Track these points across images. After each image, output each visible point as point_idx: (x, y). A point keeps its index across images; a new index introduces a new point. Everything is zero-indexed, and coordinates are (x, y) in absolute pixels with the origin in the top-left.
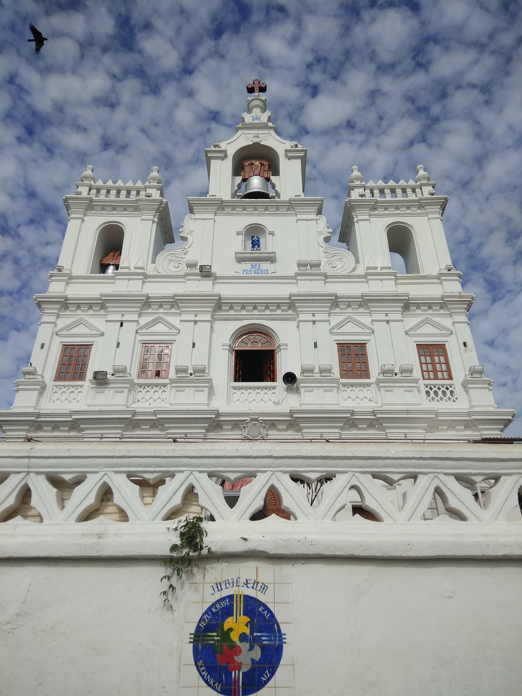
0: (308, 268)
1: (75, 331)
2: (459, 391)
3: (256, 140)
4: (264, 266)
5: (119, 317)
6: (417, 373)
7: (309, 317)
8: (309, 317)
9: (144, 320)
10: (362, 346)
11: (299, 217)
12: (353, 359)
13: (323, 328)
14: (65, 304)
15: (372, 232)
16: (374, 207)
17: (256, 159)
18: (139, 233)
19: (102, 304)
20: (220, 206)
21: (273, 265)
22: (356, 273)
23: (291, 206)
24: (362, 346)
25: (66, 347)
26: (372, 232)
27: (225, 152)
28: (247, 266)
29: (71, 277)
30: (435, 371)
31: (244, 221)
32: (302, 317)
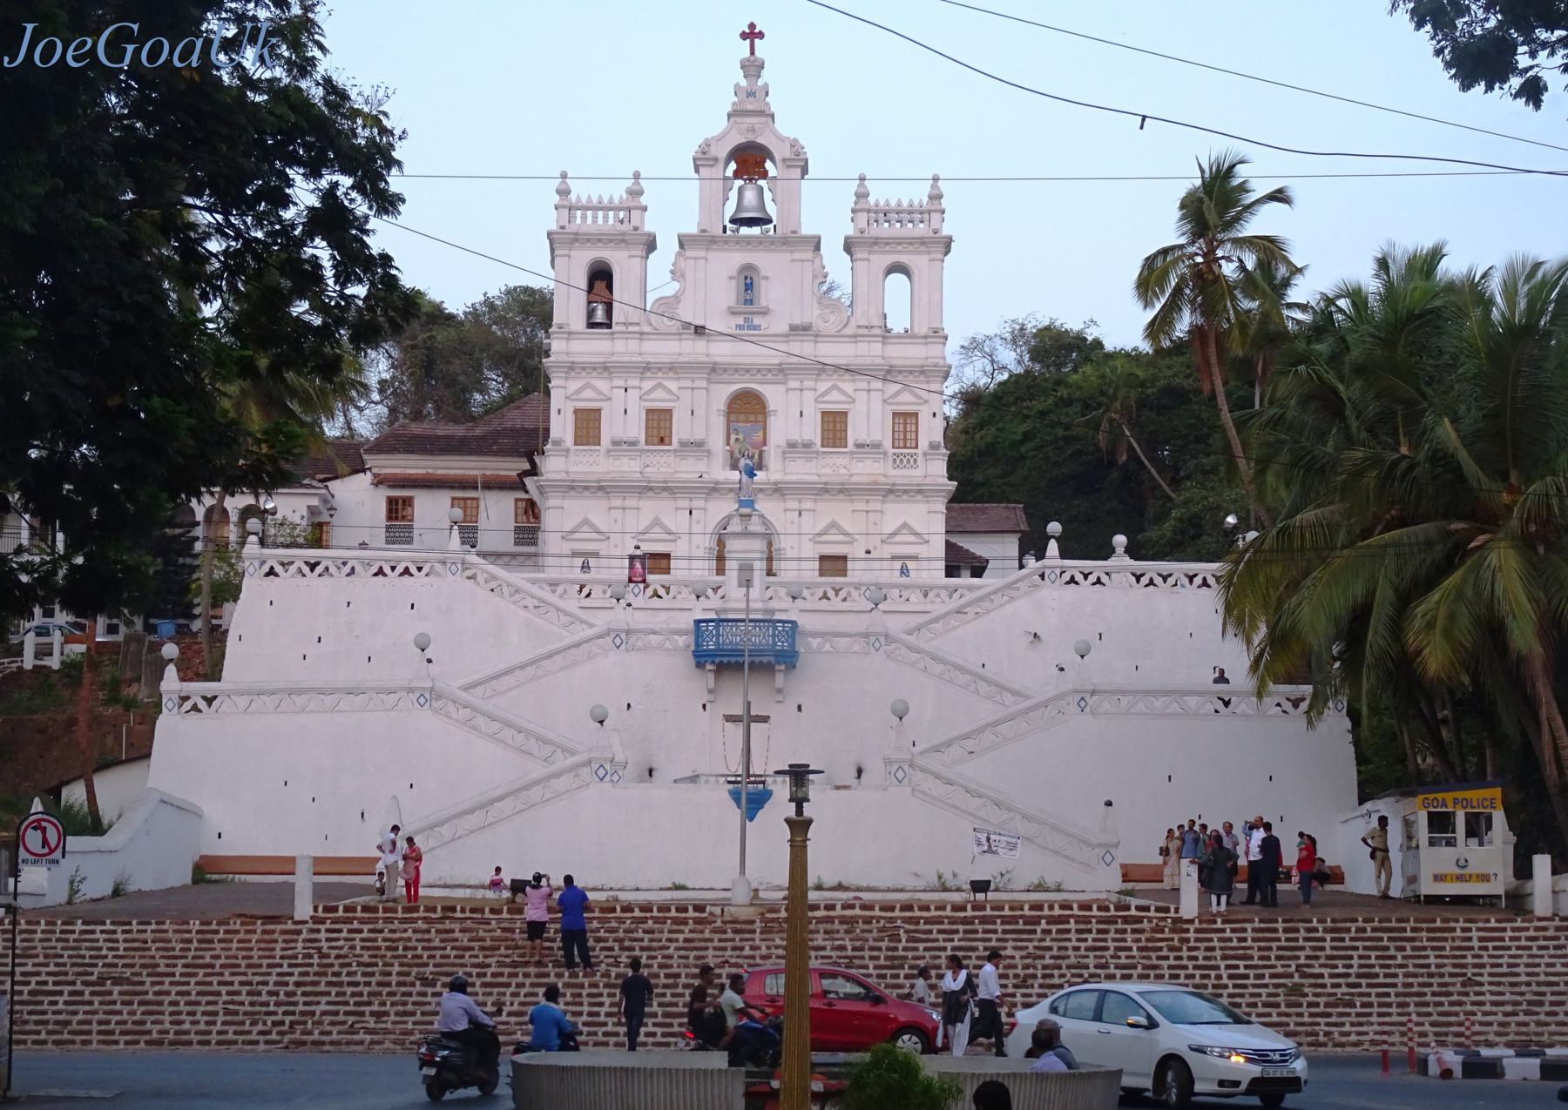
0: (800, 330)
1: (584, 395)
3: (751, 137)
4: (757, 320)
5: (621, 383)
6: (888, 444)
8: (796, 384)
9: (647, 385)
10: (844, 414)
11: (798, 256)
12: (834, 426)
13: (809, 396)
14: (572, 368)
21: (768, 318)
22: (844, 332)
24: (844, 414)
27: (716, 160)
28: (740, 321)
29: (570, 333)
30: (905, 439)
31: (739, 258)
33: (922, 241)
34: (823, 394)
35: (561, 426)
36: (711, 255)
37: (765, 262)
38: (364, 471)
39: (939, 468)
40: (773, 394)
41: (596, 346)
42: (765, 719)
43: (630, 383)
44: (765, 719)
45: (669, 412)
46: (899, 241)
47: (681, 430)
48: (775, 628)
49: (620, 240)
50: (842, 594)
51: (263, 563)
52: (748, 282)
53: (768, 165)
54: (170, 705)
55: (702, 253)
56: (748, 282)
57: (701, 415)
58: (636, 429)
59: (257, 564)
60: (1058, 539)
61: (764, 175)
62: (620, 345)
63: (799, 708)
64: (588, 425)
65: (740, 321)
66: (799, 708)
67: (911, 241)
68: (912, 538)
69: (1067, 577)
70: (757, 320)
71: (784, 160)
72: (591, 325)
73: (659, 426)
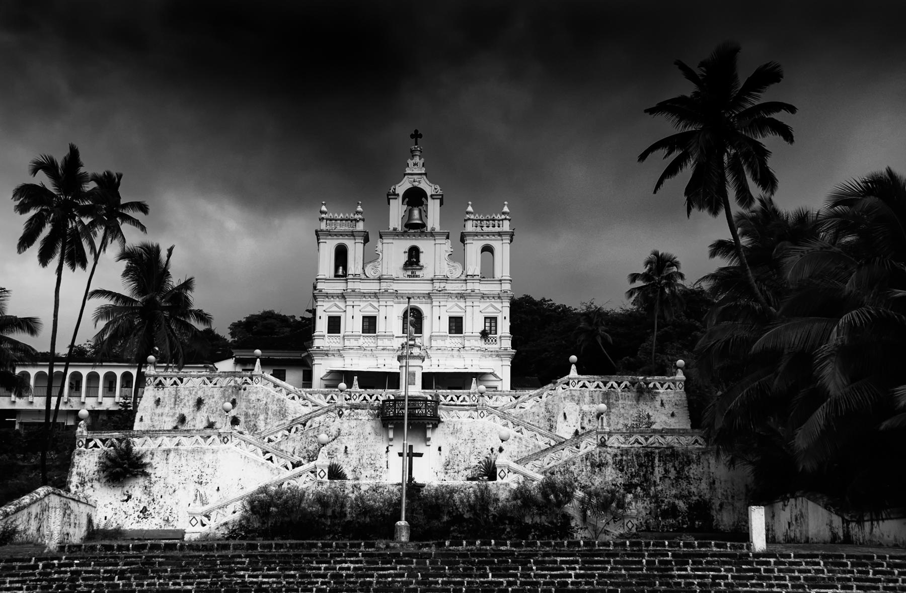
2: (498, 340)
3: (416, 184)
4: (418, 273)
7: (438, 304)
9: (363, 304)
11: (437, 242)
12: (456, 325)
14: (327, 296)
15: (474, 248)
16: (476, 234)
17: (415, 198)
18: (355, 250)
19: (343, 296)
20: (395, 234)
23: (433, 234)
25: (330, 318)
26: (474, 248)
27: (398, 195)
28: (409, 273)
32: (434, 304)
33: (500, 234)
34: (451, 308)
35: (322, 326)
36: (394, 241)
37: (423, 244)
38: (232, 357)
39: (507, 344)
40: (425, 308)
41: (338, 287)
42: (420, 455)
43: (355, 303)
44: (420, 455)
45: (375, 317)
46: (488, 234)
47: (381, 326)
48: (426, 404)
49: (352, 235)
50: (461, 398)
51: (156, 378)
52: (414, 254)
53: (423, 199)
54: (80, 444)
55: (391, 241)
56: (414, 254)
57: (391, 318)
58: (358, 326)
59: (152, 379)
60: (576, 364)
61: (421, 204)
62: (351, 285)
63: (440, 449)
64: (334, 325)
65: (409, 273)
66: (440, 449)
67: (493, 234)
68: (494, 378)
69: (581, 384)
70: (418, 273)
71: (432, 196)
72: (336, 276)
73: (370, 324)
